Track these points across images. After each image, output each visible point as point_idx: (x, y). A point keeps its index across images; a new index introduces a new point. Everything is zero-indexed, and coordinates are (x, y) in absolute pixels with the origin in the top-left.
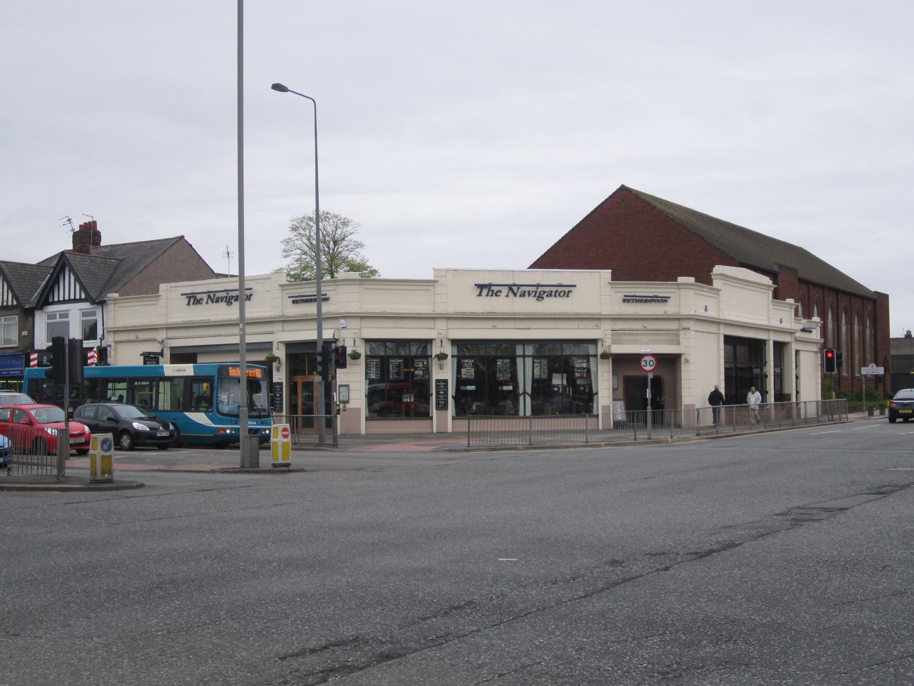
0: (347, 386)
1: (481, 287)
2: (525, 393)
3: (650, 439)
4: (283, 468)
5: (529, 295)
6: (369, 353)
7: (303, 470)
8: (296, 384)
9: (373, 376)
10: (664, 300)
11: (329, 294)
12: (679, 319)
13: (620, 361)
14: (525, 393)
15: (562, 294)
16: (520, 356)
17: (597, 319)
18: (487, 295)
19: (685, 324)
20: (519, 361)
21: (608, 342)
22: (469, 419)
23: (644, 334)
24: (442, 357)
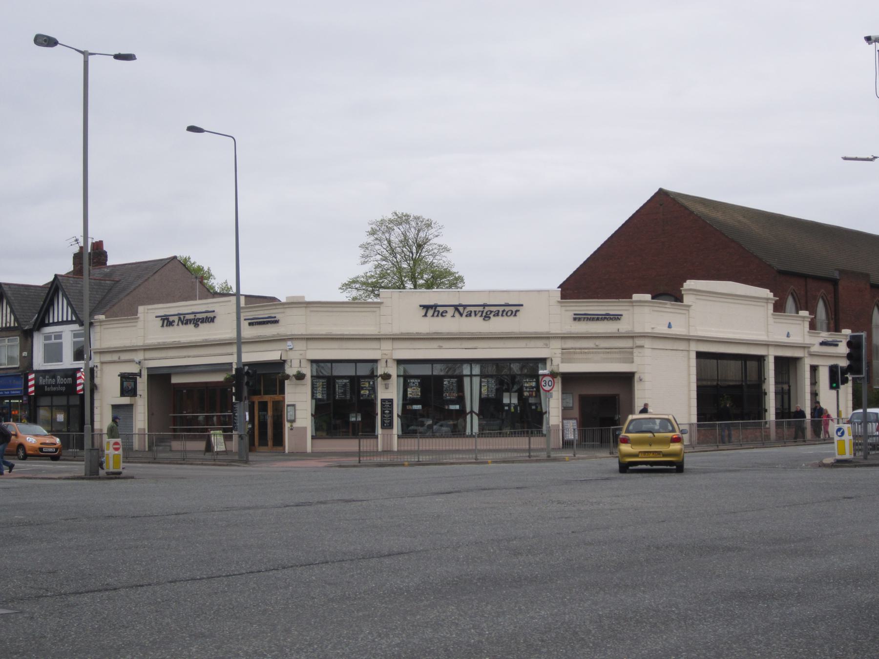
0: (294, 405)
1: (427, 308)
2: (472, 412)
3: (549, 456)
4: (116, 476)
5: (476, 315)
6: (315, 374)
7: (132, 478)
8: (253, 403)
9: (319, 396)
10: (617, 318)
11: (278, 317)
12: (632, 337)
13: (569, 380)
14: (472, 412)
16: (475, 375)
17: (545, 337)
18: (433, 316)
19: (639, 342)
20: (467, 381)
21: (557, 361)
22: (359, 439)
23: (596, 353)
24: (386, 377)
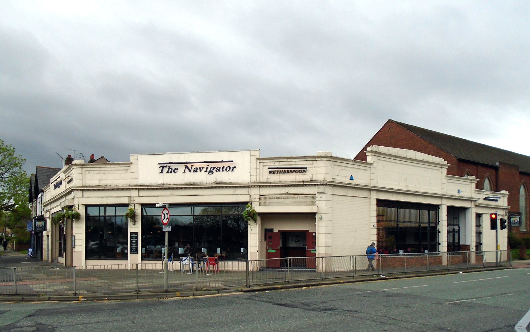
5: (200, 171)
15: (228, 169)
18: (168, 172)
19: (321, 189)
